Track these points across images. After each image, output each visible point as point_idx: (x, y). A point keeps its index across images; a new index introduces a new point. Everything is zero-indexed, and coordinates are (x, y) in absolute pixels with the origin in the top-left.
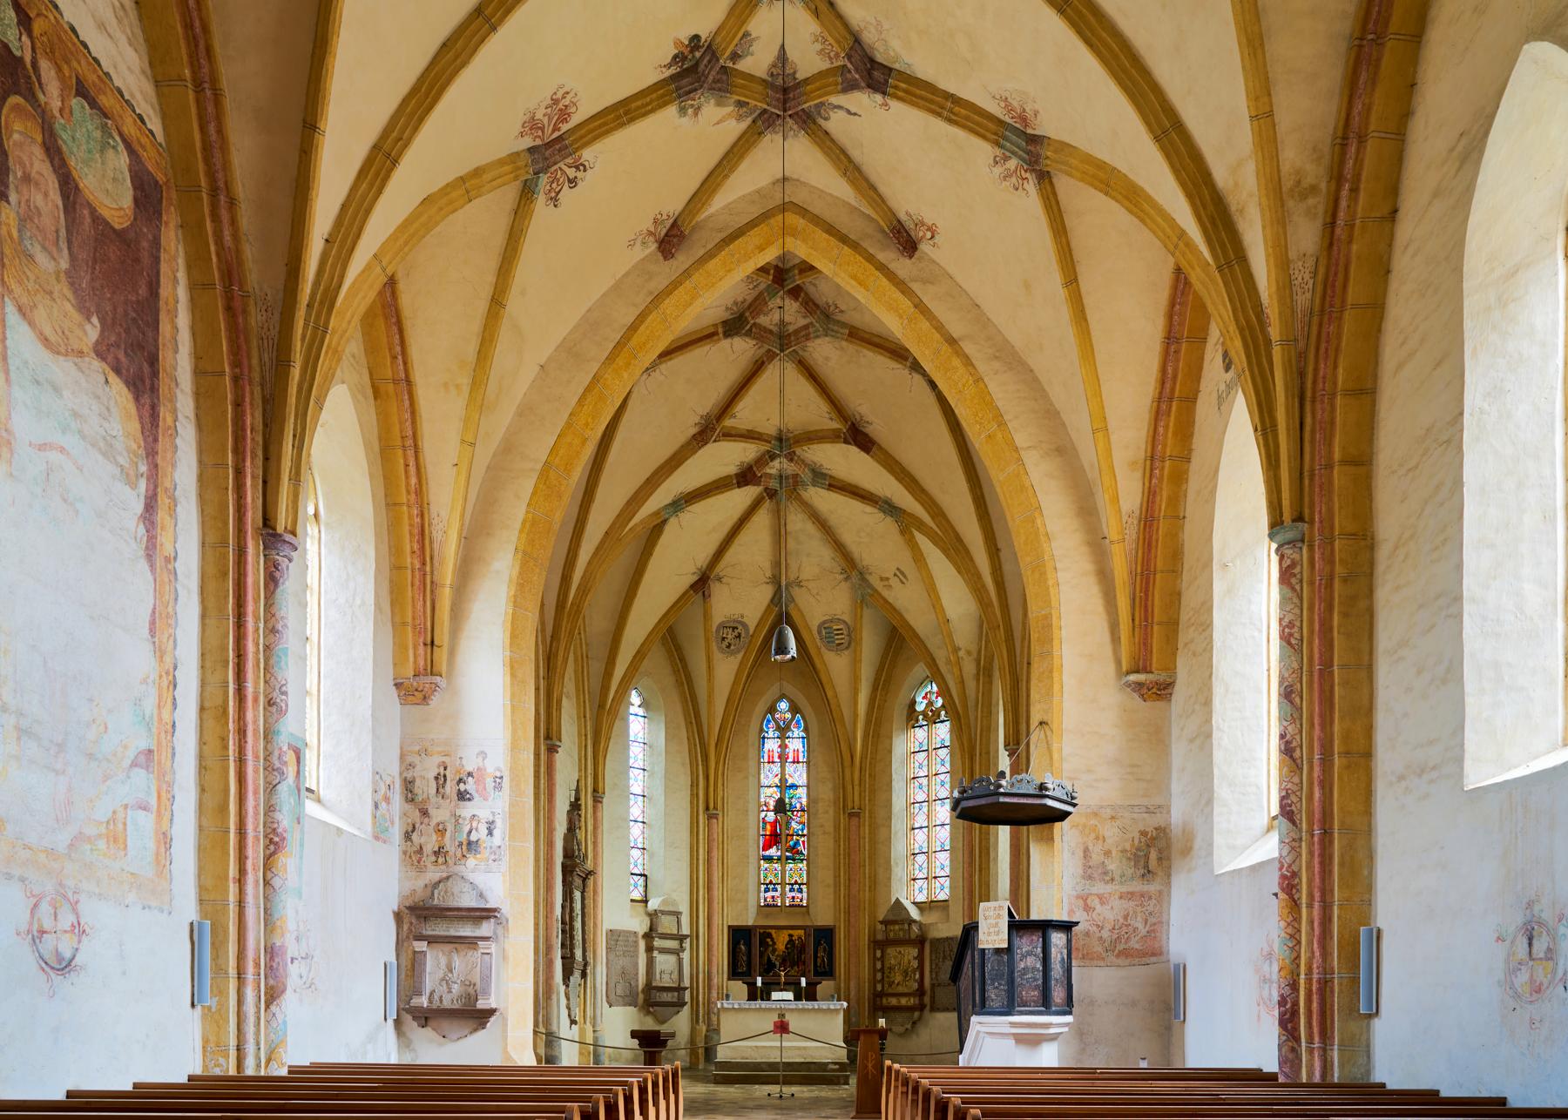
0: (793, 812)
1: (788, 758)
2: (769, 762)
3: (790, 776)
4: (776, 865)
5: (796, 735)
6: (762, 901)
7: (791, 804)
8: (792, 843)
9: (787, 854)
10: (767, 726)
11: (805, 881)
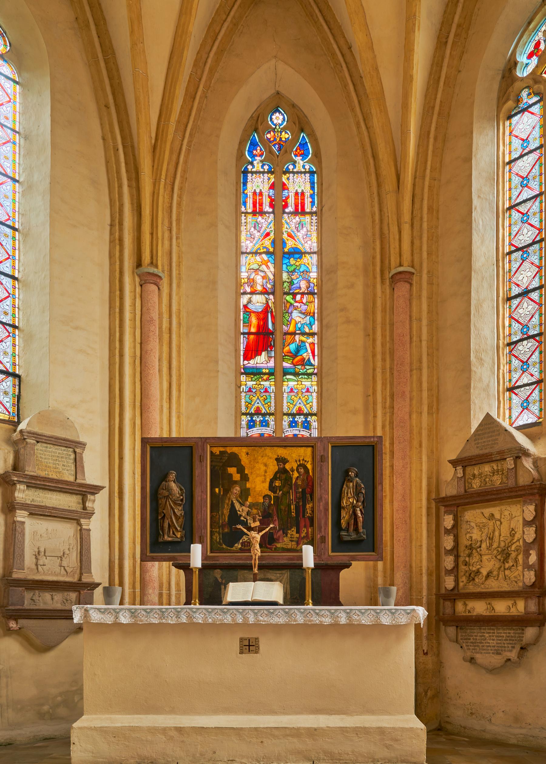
0: (294, 295)
1: (286, 206)
2: (254, 213)
3: (290, 235)
4: (266, 384)
5: (299, 167)
7: (291, 283)
8: (293, 347)
9: (285, 364)
10: (250, 152)
11: (315, 410)
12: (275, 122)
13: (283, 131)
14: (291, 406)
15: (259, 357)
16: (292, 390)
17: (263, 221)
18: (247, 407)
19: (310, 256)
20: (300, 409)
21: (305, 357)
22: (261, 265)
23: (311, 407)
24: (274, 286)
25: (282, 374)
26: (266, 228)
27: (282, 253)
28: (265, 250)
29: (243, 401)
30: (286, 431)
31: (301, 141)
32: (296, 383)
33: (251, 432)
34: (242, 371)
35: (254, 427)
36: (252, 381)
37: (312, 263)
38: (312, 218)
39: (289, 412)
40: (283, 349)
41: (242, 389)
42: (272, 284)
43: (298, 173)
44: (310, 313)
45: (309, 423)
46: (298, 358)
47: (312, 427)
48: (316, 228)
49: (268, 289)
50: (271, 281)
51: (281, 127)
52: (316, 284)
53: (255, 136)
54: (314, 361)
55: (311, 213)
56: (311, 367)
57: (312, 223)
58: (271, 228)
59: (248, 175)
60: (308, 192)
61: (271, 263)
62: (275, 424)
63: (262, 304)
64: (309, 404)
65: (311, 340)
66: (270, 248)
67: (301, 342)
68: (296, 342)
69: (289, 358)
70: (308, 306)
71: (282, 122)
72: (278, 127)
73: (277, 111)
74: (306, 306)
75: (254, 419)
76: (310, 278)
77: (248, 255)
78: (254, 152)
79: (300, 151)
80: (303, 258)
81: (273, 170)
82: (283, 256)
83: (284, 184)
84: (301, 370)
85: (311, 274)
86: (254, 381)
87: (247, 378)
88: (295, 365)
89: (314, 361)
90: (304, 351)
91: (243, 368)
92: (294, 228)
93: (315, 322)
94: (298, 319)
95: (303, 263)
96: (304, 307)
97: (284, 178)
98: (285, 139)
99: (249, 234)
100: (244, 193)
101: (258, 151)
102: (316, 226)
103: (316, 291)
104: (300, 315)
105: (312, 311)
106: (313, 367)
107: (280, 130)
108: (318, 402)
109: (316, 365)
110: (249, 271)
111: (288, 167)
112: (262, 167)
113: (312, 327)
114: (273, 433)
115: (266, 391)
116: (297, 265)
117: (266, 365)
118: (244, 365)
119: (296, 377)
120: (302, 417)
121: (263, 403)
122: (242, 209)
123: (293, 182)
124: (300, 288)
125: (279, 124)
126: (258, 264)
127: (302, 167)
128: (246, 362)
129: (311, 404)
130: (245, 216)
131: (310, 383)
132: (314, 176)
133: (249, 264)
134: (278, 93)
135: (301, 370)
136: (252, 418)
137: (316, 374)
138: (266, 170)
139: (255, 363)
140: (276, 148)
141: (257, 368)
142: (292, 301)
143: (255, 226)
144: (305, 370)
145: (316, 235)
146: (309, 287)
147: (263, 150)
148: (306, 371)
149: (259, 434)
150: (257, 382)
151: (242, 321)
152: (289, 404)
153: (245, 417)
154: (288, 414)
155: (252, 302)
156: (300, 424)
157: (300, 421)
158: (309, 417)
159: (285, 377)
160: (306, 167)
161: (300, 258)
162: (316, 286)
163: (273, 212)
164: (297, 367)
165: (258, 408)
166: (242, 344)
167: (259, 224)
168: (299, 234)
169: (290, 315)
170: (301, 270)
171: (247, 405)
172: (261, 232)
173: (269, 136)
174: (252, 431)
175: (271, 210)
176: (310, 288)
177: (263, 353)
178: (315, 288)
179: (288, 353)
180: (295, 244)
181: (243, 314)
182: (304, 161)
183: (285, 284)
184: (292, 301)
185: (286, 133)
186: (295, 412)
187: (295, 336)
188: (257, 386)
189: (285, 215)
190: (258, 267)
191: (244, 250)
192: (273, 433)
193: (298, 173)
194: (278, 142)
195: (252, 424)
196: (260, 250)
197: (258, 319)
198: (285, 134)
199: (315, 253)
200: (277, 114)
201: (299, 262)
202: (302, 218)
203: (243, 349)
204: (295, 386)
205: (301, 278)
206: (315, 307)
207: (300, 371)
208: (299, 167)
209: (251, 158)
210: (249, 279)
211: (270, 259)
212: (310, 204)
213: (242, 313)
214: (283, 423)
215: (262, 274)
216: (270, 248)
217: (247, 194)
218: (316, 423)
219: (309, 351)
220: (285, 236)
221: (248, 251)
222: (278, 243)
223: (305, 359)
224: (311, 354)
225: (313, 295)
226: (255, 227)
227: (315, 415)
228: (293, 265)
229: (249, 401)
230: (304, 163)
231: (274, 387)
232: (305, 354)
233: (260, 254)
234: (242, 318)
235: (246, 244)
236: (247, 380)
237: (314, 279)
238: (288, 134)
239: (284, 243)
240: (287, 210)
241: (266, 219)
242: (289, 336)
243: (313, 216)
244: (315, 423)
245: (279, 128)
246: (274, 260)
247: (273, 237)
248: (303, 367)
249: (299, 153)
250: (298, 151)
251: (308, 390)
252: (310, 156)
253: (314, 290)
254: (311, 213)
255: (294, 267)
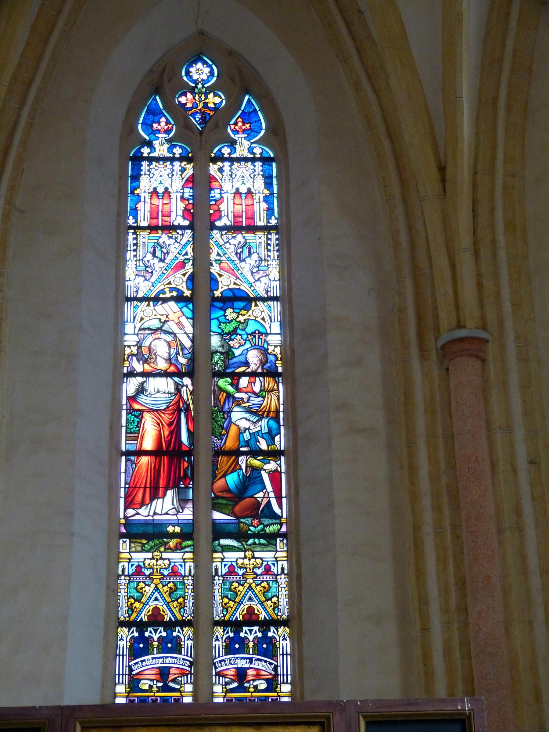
0: (235, 377)
2: (152, 228)
4: (176, 556)
5: (242, 150)
6: (121, 689)
7: (228, 354)
8: (232, 479)
9: (218, 516)
10: (147, 125)
11: (284, 612)
12: (195, 77)
13: (209, 93)
14: (231, 604)
15: (160, 500)
16: (232, 571)
17: (172, 241)
18: (131, 608)
19: (266, 304)
20: (250, 610)
21: (260, 500)
22: (166, 321)
23: (276, 606)
24: (192, 360)
25: (211, 536)
26: (178, 255)
27: (209, 299)
28: (174, 294)
29: (123, 594)
30: (220, 662)
31: (245, 108)
32: (242, 555)
33: (140, 665)
34: (123, 530)
35: (148, 654)
36: (143, 551)
37: (270, 317)
38: (269, 236)
39: (227, 618)
40: (213, 483)
41: (120, 569)
42: (189, 356)
43: (239, 160)
44: (269, 412)
45: (271, 642)
46: (247, 502)
47: (280, 651)
48: (276, 254)
49: (179, 366)
50: (187, 352)
51: (206, 86)
52: (279, 356)
53: (156, 100)
54: (281, 507)
55: (267, 229)
56: (274, 521)
57: (270, 245)
58: (186, 254)
59: (143, 163)
60: (259, 192)
61: (187, 318)
62: (196, 645)
63: (167, 395)
64: (270, 599)
65: (272, 466)
66: (185, 289)
67: (250, 470)
68: (240, 468)
69: (224, 502)
70: (264, 397)
71: (208, 77)
72: (200, 86)
73: (198, 59)
74: (260, 399)
75: (147, 634)
76: (268, 344)
77: (139, 304)
78: (155, 126)
79: (243, 125)
80: (253, 307)
81: (190, 155)
82: (212, 305)
83: (212, 179)
84: (252, 528)
85: (269, 338)
86: (148, 551)
87: (132, 545)
88: (238, 518)
89: (281, 507)
90: (259, 487)
91: (125, 525)
92: (234, 254)
93: (280, 429)
94: (244, 424)
95: (252, 317)
96: (255, 400)
97: (213, 169)
98: (215, 104)
99: (141, 264)
100: (132, 193)
101: (163, 124)
102: (278, 251)
103: (280, 370)
104: (247, 415)
105: (273, 408)
106: (278, 521)
107: (204, 90)
108: (290, 596)
109: (284, 516)
110: (142, 332)
111: (220, 150)
112: (170, 150)
113: (273, 439)
114: (190, 666)
115: (174, 572)
116: (240, 322)
117: (174, 518)
118: (125, 517)
119: (240, 542)
120: (256, 628)
121: (168, 599)
122: (128, 221)
123: (231, 176)
124: (247, 364)
125: (203, 80)
126: (160, 320)
127: (246, 151)
128: (130, 512)
129: (275, 599)
130: (134, 233)
131: (272, 554)
132: (271, 166)
133: (142, 319)
134: (201, 33)
135: (252, 528)
136: (141, 633)
137: (284, 536)
138: (177, 155)
139: (151, 514)
140: (197, 119)
141: (154, 524)
142: (231, 389)
143: (154, 251)
144: (261, 527)
145: (277, 266)
146: (267, 362)
147: (173, 123)
148: (263, 530)
149: (158, 668)
150: (155, 553)
151: (124, 429)
152: (226, 600)
153: (125, 630)
154: (223, 624)
155: (147, 391)
156: (251, 644)
157: (251, 640)
158: (272, 628)
159: (217, 542)
160: (255, 150)
161: (247, 308)
162: (281, 360)
163: (191, 227)
164: (242, 520)
165: (156, 609)
166: (123, 476)
167: (162, 248)
168: (243, 264)
169: (226, 416)
170: (249, 330)
171: (132, 604)
172: (166, 261)
173: (183, 100)
174: (142, 661)
175: (186, 223)
176: (268, 365)
177: (169, 493)
178: (279, 363)
179: (222, 492)
180: (235, 284)
181: (127, 414)
182: (252, 141)
183: (216, 357)
184: (231, 389)
185: (216, 94)
186: (240, 618)
187: (237, 457)
188: (154, 562)
189: (215, 232)
190: (159, 325)
191: (131, 293)
192: (190, 666)
193: (239, 160)
194: (200, 110)
195: (141, 646)
196: (165, 293)
197: (158, 424)
198: (215, 96)
199: (274, 299)
200: (200, 65)
201: (244, 315)
202: (250, 237)
203: (126, 483)
204: (240, 562)
205: (248, 345)
206: (278, 399)
207: (250, 530)
208: (242, 150)
209: (148, 135)
210: (139, 346)
211: (185, 310)
212: (264, 215)
213: (124, 413)
214: (214, 643)
215: (169, 338)
216: (185, 289)
217: (138, 195)
218: (288, 642)
219: (269, 487)
220: (215, 269)
221: (140, 295)
222: (202, 281)
223: (259, 504)
224: (272, 495)
225: (274, 377)
226: (154, 254)
227: (285, 623)
228: (231, 321)
229: (136, 594)
230: (252, 143)
231: (192, 564)
232: (261, 494)
233: (165, 300)
234: (124, 423)
235: (135, 283)
236: (133, 550)
237: (276, 346)
238: (220, 97)
239: (213, 281)
240: (218, 223)
241: (176, 238)
242: (225, 459)
243: (271, 234)
244: (284, 643)
245: (203, 87)
246: (193, 311)
247: (191, 270)
248: (256, 522)
249: (241, 128)
250: (240, 124)
251: (268, 571)
252: (263, 132)
253: (277, 367)
254: (267, 229)
255: (234, 324)
